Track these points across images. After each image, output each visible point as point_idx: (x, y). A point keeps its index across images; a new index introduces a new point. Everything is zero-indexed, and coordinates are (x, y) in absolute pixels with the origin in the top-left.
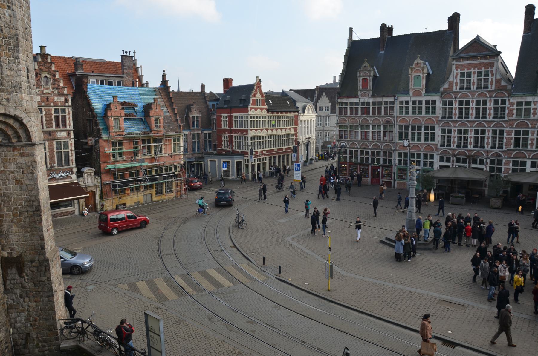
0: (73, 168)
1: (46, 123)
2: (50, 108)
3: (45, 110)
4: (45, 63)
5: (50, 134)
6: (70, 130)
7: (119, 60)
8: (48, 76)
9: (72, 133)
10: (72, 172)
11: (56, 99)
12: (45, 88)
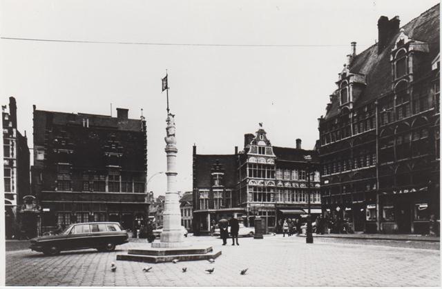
0: (13, 195)
6: (13, 160)
7: (115, 115)
9: (15, 162)
10: (13, 199)
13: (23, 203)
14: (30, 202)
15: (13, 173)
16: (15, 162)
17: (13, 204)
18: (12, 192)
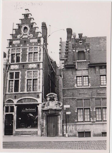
0: (39, 93)
1: (22, 58)
2: (26, 47)
3: (22, 49)
4: (26, 19)
5: (24, 66)
6: (40, 63)
8: (28, 26)
9: (41, 65)
10: (38, 97)
11: (31, 41)
12: (24, 35)
13: (47, 101)
14: (52, 99)
15: (40, 74)
16: (41, 65)
17: (39, 103)
18: (38, 91)
